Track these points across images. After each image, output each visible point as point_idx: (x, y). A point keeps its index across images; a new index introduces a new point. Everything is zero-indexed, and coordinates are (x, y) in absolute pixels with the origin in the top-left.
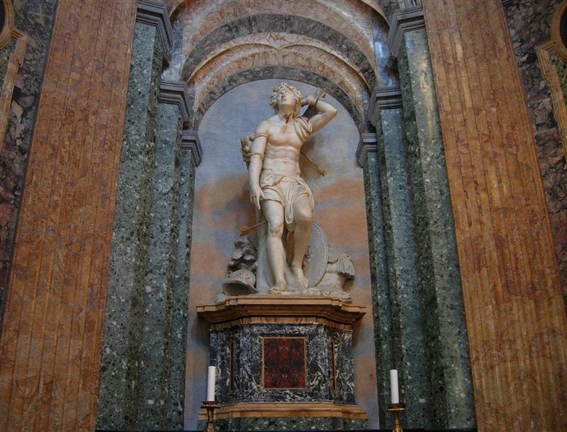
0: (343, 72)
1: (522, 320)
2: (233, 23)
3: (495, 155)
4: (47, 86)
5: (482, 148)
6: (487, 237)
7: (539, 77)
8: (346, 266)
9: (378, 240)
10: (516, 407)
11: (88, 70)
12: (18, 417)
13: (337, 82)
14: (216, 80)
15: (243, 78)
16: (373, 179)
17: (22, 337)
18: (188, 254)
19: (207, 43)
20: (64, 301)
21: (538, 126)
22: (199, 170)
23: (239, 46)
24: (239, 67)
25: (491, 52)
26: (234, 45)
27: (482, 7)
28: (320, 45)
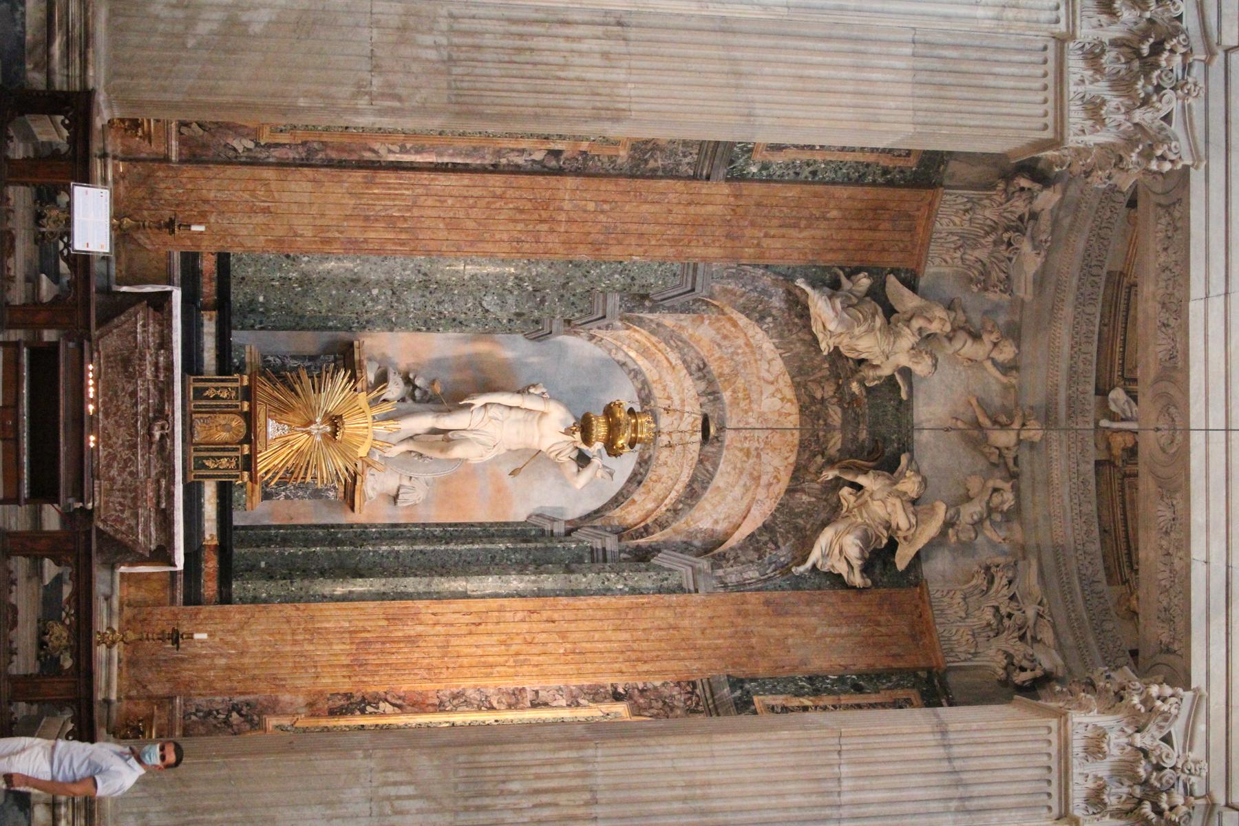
0: (650, 506)
4: (570, 182)
5: (518, 634)
6: (419, 629)
7: (594, 701)
8: (406, 496)
10: (250, 639)
11: (602, 218)
12: (236, 187)
13: (636, 497)
17: (310, 184)
18: (419, 330)
20: (347, 217)
21: (537, 692)
28: (685, 478)
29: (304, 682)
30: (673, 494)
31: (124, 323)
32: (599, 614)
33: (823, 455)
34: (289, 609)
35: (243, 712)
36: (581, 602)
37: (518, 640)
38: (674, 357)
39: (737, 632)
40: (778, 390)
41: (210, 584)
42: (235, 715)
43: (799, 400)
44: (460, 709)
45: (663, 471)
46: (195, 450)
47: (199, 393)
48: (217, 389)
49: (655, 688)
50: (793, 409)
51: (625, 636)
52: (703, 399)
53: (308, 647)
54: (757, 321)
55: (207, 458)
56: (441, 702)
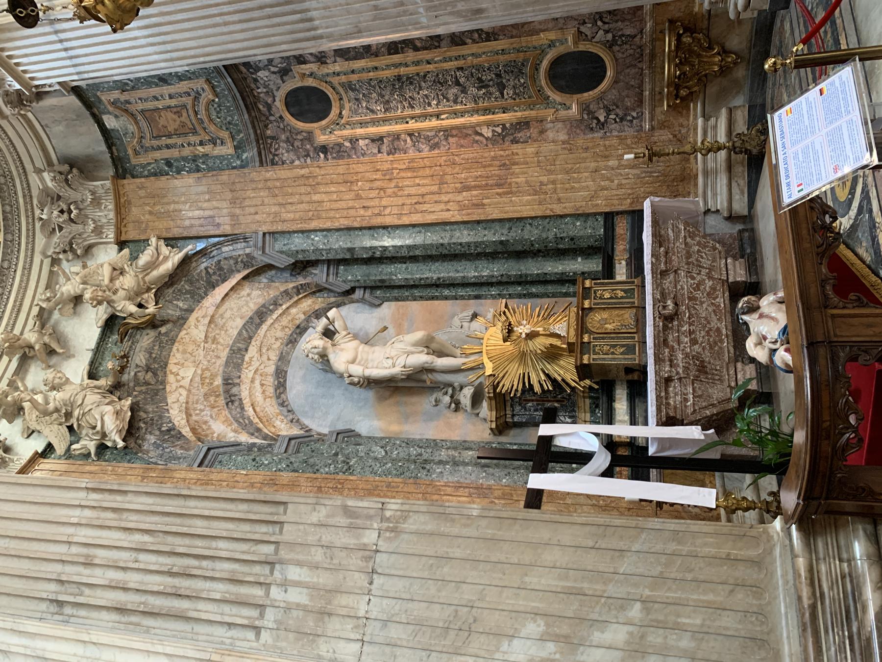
0: (293, 311)
1: (526, 175)
2: (226, 399)
3: (397, 187)
5: (390, 196)
6: (460, 198)
7: (340, 145)
9: (446, 292)
13: (303, 317)
14: (279, 417)
15: (283, 395)
16: (395, 293)
19: (241, 421)
21: (379, 152)
22: (363, 435)
23: (250, 396)
24: (271, 397)
25: (311, 180)
26: (248, 400)
27: (269, 184)
28: (264, 327)
29: (547, 148)
30: (275, 316)
31: (706, 407)
32: (332, 214)
33: (160, 333)
34: (558, 209)
35: (595, 121)
36: (344, 223)
37: (389, 191)
38: (250, 412)
39: (241, 203)
40: (178, 381)
41: (622, 232)
42: (602, 119)
43: (165, 373)
44: (433, 133)
45: (279, 334)
46: (634, 303)
47: (630, 349)
48: (613, 353)
49: (299, 159)
50: (172, 367)
51: (316, 197)
52: (237, 381)
53: (544, 179)
54: (174, 429)
55: (622, 297)
56: (446, 139)
